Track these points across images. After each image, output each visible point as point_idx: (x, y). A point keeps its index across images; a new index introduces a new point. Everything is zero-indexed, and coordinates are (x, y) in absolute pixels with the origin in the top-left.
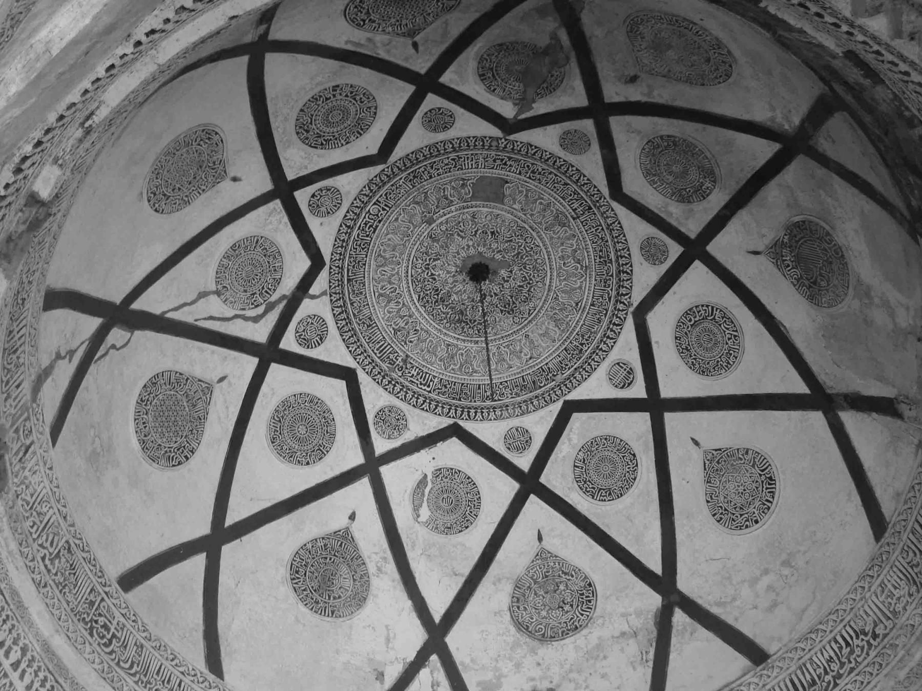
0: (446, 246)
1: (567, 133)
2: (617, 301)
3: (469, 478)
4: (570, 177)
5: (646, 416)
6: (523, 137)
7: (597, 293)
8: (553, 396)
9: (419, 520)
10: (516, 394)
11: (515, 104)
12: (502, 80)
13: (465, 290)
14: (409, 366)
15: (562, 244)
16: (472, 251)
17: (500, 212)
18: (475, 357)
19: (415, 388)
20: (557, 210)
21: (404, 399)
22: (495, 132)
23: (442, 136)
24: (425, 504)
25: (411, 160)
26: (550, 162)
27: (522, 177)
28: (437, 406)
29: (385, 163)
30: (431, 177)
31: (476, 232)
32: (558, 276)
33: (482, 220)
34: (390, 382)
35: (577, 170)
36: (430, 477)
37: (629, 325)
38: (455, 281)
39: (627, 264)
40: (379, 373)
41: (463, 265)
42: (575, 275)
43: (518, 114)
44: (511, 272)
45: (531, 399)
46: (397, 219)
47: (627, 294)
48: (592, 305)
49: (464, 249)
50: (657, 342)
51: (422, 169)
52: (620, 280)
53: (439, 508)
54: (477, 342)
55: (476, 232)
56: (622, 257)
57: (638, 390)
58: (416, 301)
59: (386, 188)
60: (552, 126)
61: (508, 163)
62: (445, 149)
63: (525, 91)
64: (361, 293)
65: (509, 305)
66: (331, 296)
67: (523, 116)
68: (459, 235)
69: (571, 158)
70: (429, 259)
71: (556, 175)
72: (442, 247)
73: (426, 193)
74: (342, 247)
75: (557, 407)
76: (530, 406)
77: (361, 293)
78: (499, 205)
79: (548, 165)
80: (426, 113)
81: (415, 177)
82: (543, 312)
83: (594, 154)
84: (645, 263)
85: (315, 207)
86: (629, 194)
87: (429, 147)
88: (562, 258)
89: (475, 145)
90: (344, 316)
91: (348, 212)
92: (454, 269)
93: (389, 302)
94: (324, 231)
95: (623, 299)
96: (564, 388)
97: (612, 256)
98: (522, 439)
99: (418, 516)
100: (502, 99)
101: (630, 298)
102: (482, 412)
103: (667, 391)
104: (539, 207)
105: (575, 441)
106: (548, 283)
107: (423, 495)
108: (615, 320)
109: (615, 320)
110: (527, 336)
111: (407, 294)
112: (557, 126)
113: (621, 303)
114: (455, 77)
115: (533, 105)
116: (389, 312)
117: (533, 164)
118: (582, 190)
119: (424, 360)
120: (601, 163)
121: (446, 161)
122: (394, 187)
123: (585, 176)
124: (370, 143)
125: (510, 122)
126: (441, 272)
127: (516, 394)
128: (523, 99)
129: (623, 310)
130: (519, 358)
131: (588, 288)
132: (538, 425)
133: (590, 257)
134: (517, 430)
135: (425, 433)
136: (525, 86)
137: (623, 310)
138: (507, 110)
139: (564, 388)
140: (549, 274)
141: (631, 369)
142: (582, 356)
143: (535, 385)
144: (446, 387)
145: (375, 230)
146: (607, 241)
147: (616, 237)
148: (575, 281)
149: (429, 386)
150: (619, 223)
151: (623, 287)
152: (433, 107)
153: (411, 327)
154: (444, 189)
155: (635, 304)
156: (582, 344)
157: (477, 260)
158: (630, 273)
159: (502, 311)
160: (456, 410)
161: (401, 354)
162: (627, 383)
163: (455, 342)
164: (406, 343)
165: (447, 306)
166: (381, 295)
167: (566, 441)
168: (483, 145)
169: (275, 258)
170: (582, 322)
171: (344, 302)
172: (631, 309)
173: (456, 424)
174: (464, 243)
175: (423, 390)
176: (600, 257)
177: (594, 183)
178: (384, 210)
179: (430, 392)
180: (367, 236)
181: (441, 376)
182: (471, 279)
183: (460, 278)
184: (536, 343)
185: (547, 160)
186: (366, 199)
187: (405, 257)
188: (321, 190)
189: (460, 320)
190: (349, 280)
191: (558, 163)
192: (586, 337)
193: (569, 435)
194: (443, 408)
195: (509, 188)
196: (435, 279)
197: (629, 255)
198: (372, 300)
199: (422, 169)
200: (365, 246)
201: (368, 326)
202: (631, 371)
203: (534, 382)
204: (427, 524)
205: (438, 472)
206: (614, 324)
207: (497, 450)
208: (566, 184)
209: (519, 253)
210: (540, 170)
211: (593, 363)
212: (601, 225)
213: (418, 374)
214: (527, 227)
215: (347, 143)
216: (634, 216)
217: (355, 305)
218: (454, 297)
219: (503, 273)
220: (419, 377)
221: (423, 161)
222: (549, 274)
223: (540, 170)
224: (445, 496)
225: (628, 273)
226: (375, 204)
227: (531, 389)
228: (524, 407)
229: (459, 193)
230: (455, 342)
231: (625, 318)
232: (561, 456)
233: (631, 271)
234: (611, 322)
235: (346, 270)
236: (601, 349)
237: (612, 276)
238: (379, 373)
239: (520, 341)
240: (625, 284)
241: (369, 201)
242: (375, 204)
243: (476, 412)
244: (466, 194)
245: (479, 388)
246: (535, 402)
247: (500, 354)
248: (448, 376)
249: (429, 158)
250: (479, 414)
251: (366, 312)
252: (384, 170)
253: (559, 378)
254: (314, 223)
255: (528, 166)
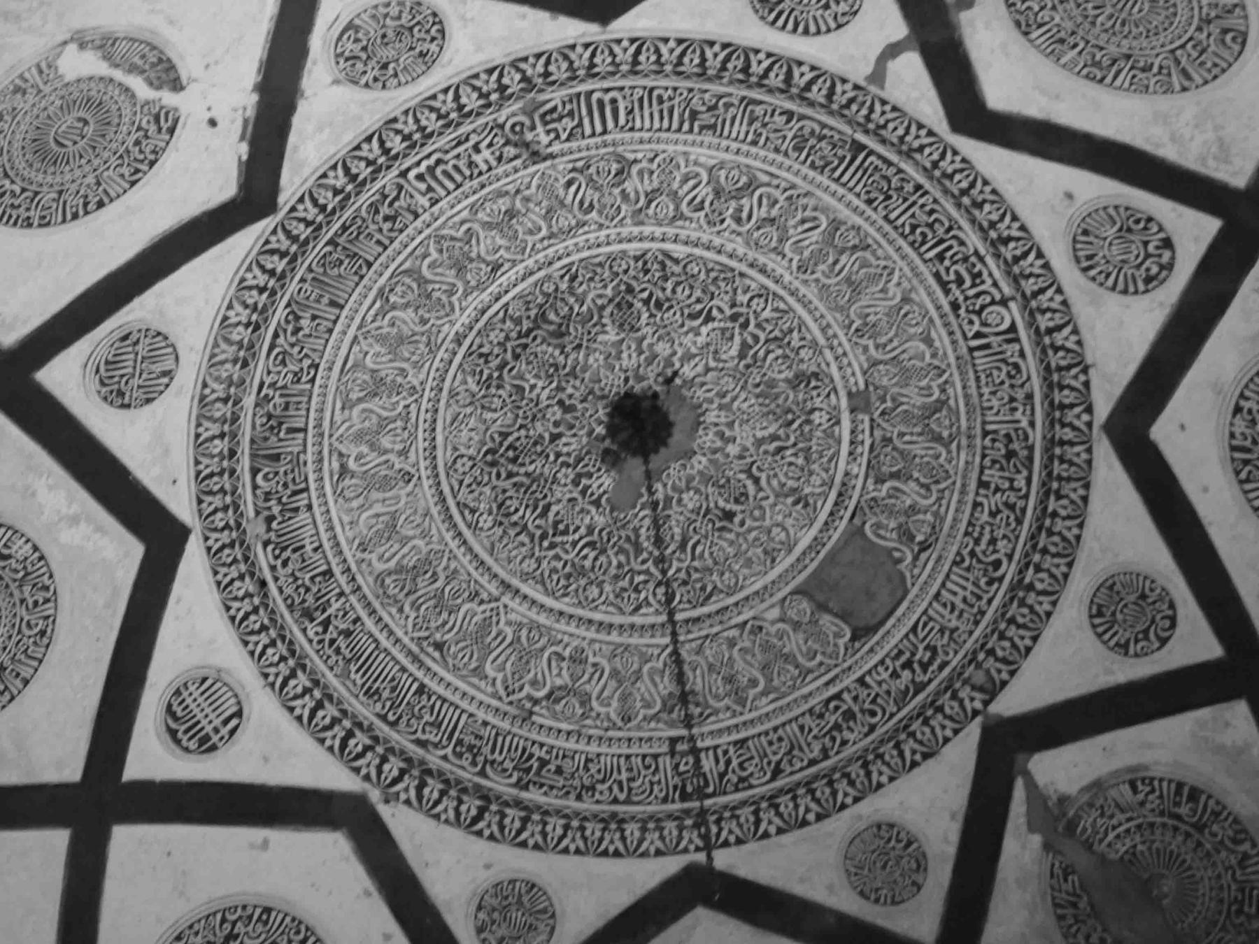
0: (767, 390)
1: (921, 864)
2: (409, 760)
3: (101, 205)
4: (791, 790)
5: (72, 772)
6: (962, 753)
7: (449, 715)
8: (217, 501)
9: (73, 47)
10: (267, 399)
11: (1063, 800)
12: (1152, 825)
13: (614, 361)
14: (510, 151)
15: (615, 673)
16: (708, 439)
17: (779, 569)
18: (424, 322)
19: (442, 142)
20: (716, 712)
21: (428, 103)
22: (1010, 704)
23: (1080, 586)
24: (103, 69)
25: (1065, 488)
26: (855, 770)
27: (849, 681)
28: (353, 178)
29: (1108, 427)
30: (982, 484)
31: (757, 481)
32: (534, 626)
33: (778, 513)
34: (502, 88)
35: (805, 823)
36: (168, 98)
37: (334, 776)
38: (649, 361)
39: (502, 827)
40: (547, 74)
41: (683, 399)
42: (518, 674)
43: (1031, 785)
44: (597, 503)
45: (234, 435)
46: (928, 341)
47: (420, 797)
48: (422, 689)
49: (726, 428)
50: (265, 844)
51: (1020, 482)
52: (464, 790)
53: (67, 107)
54: (458, 342)
55: (757, 481)
56: (525, 821)
57: (150, 757)
58: (668, 246)
59: (1036, 385)
60: (954, 836)
61: (906, 675)
62: (1038, 569)
63: (1088, 846)
64: (798, 149)
65: (514, 460)
66: (856, 87)
67: (1019, 784)
68: (774, 437)
69: (840, 826)
70: (761, 336)
71: (812, 763)
72: (772, 384)
73: (947, 446)
74: (964, 192)
75: (180, 502)
76: (215, 429)
77: (798, 149)
78: (801, 578)
79: (850, 761)
80: (1172, 606)
81: (1010, 455)
82: (453, 544)
83: (830, 888)
84: (485, 879)
85: (1134, 225)
86: (687, 920)
87: (1069, 551)
88: (578, 659)
89: (1002, 637)
90: (775, 80)
91: (1046, 266)
92: (687, 371)
93: (718, 193)
94: (1045, 195)
95: (410, 782)
96: (225, 537)
97: (533, 796)
98: (135, 382)
99: (82, 46)
100: (1097, 786)
101: (408, 802)
102: (262, 290)
103: (126, 841)
104: (746, 670)
105: (69, 536)
106: (525, 589)
107: (133, 69)
108: (361, 739)
109: (361, 739)
110: (407, 477)
111: (705, 238)
112: (952, 850)
113: (402, 772)
114: (1228, 738)
115: (1036, 840)
116: (686, 179)
117: (872, 728)
118: (744, 803)
119: (501, 194)
120: (799, 890)
121: (1001, 544)
122: (1020, 395)
123: (780, 831)
124: (1190, 433)
125: (1020, 757)
126: (701, 340)
127: (267, 399)
128: (1071, 827)
129: (380, 772)
130: (359, 437)
131: (473, 696)
132: (155, 443)
133: (552, 732)
134: (167, 373)
135: (297, 120)
136: (1103, 858)
137: (380, 772)
138: (1061, 769)
139: (225, 537)
140: (549, 602)
141: (214, 748)
142: (291, 614)
143: (265, 457)
144: (386, 219)
145: (944, 286)
146: (579, 798)
147: (582, 829)
148: (502, 668)
149: (420, 177)
150: (617, 854)
151: (443, 793)
152: (1179, 631)
153: (607, 200)
154: (927, 487)
155: (384, 811)
156: (326, 624)
157: (677, 437)
158: (472, 826)
159: (504, 435)
160: (308, 224)
161: (556, 148)
162: (184, 730)
163: (494, 288)
164: (574, 170)
165: (602, 308)
166: (752, 185)
167: (75, 509)
168: (991, 652)
169: (1097, 64)
170: (385, 643)
171: (812, 104)
172: (375, 795)
173: (269, 207)
174: (744, 436)
175: (418, 162)
176: (543, 763)
177: (751, 846)
178: (978, 335)
179: (404, 174)
180: (941, 257)
181: (426, 217)
182: (628, 395)
183: (651, 372)
184: (375, 495)
185: (865, 765)
186: (1044, 322)
187: (810, 293)
188: (1170, 267)
189: (545, 322)
190: (858, 147)
191: (842, 786)
192: (342, 642)
193: (89, 520)
194: (336, 192)
195: (838, 635)
196: (693, 316)
197: (523, 844)
198: (758, 160)
199: (1020, 482)
200: (917, 237)
201: (694, 115)
202: (207, 746)
203: (276, 458)
204: (47, 68)
205: (167, 123)
206: (350, 734)
207: (136, 302)
208: (777, 772)
209: (638, 549)
210: (847, 735)
211: (264, 639)
212: (628, 801)
213: (471, 164)
214: (705, 610)
215: (1238, 410)
216: (622, 900)
217: (780, 120)
218: (612, 335)
219: (605, 481)
220: (462, 164)
221: (1043, 502)
222: (549, 602)
223: (847, 735)
224: (89, 130)
225: (475, 820)
226: (1013, 328)
227: (259, 439)
228: (220, 410)
229: (891, 512)
230: (494, 288)
231: (357, 770)
232: (40, 485)
233: (479, 833)
234: (359, 725)
235: (894, 158)
236: (293, 674)
237: (482, 773)
238: (547, 74)
239: (404, 453)
240: (448, 804)
241: (1031, 323)
242: (1013, 328)
243: (272, 273)
244: (878, 526)
245: (333, 304)
246: (219, 446)
247: (397, 389)
248: (414, 234)
249: (1039, 519)
250: (262, 279)
251: (740, 128)
252: (1089, 410)
253: (255, 529)
254: (1093, 187)
255: (873, 714)
